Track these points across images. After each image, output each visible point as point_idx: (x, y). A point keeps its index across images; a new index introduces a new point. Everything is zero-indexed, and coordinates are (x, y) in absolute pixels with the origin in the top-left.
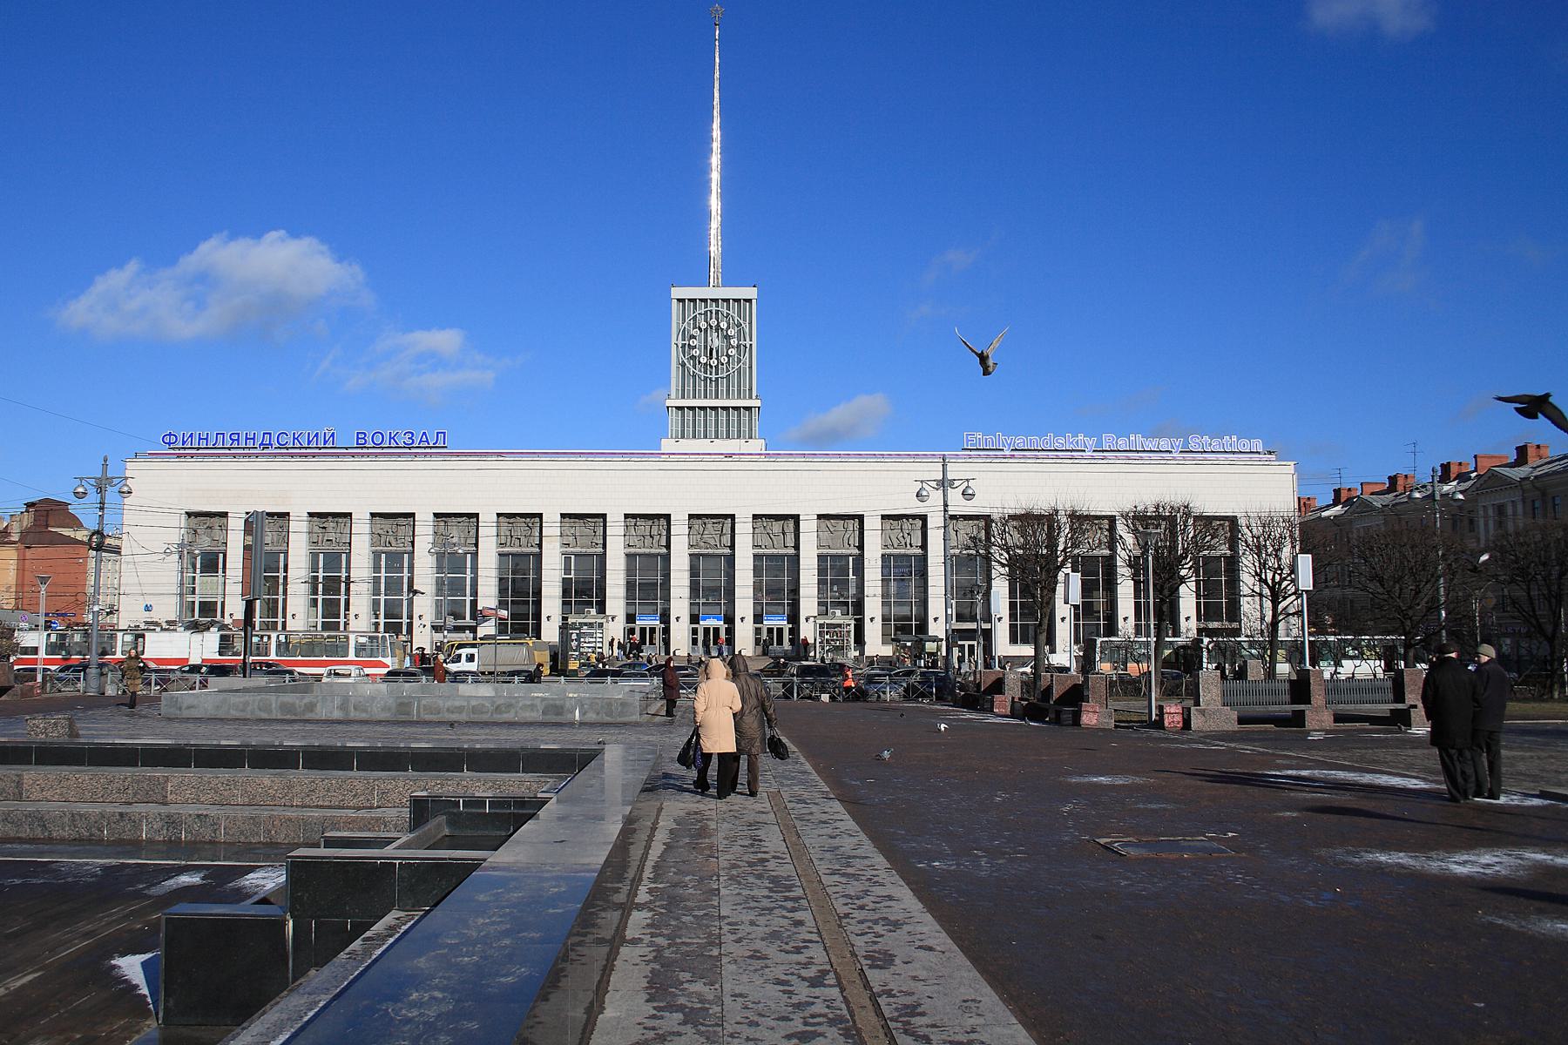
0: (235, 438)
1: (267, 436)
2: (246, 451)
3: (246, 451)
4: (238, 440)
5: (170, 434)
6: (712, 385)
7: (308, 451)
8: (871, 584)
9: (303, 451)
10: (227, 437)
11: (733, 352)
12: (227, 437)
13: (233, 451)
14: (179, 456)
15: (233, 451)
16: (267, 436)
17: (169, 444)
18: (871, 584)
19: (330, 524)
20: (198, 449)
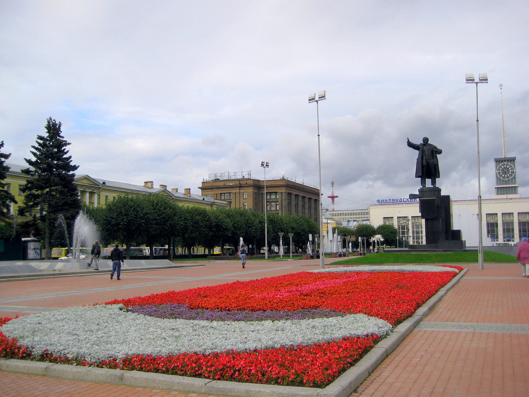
0: (393, 200)
1: (401, 200)
2: (396, 203)
3: (396, 203)
4: (394, 201)
5: (379, 200)
6: (506, 182)
7: (410, 202)
8: (499, 225)
9: (409, 202)
10: (392, 200)
11: (510, 173)
12: (392, 200)
13: (393, 203)
14: (381, 205)
15: (393, 203)
16: (401, 200)
17: (378, 202)
18: (499, 225)
19: (416, 219)
20: (385, 203)
